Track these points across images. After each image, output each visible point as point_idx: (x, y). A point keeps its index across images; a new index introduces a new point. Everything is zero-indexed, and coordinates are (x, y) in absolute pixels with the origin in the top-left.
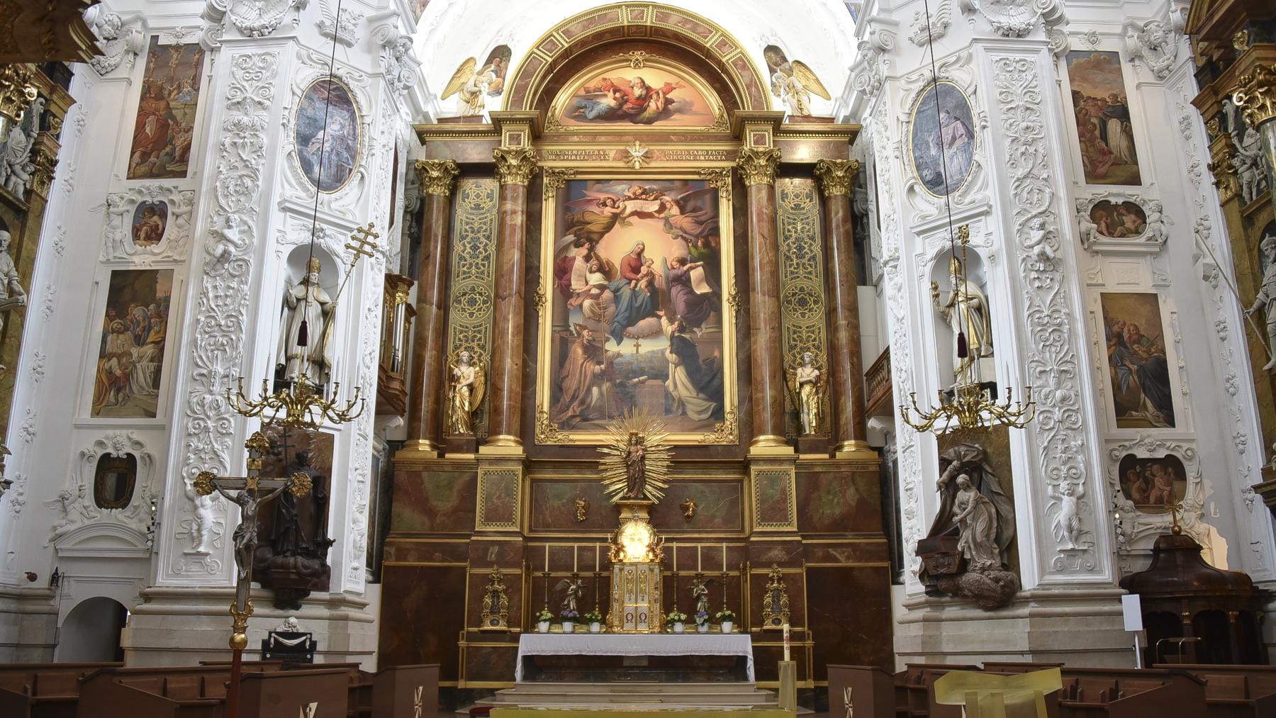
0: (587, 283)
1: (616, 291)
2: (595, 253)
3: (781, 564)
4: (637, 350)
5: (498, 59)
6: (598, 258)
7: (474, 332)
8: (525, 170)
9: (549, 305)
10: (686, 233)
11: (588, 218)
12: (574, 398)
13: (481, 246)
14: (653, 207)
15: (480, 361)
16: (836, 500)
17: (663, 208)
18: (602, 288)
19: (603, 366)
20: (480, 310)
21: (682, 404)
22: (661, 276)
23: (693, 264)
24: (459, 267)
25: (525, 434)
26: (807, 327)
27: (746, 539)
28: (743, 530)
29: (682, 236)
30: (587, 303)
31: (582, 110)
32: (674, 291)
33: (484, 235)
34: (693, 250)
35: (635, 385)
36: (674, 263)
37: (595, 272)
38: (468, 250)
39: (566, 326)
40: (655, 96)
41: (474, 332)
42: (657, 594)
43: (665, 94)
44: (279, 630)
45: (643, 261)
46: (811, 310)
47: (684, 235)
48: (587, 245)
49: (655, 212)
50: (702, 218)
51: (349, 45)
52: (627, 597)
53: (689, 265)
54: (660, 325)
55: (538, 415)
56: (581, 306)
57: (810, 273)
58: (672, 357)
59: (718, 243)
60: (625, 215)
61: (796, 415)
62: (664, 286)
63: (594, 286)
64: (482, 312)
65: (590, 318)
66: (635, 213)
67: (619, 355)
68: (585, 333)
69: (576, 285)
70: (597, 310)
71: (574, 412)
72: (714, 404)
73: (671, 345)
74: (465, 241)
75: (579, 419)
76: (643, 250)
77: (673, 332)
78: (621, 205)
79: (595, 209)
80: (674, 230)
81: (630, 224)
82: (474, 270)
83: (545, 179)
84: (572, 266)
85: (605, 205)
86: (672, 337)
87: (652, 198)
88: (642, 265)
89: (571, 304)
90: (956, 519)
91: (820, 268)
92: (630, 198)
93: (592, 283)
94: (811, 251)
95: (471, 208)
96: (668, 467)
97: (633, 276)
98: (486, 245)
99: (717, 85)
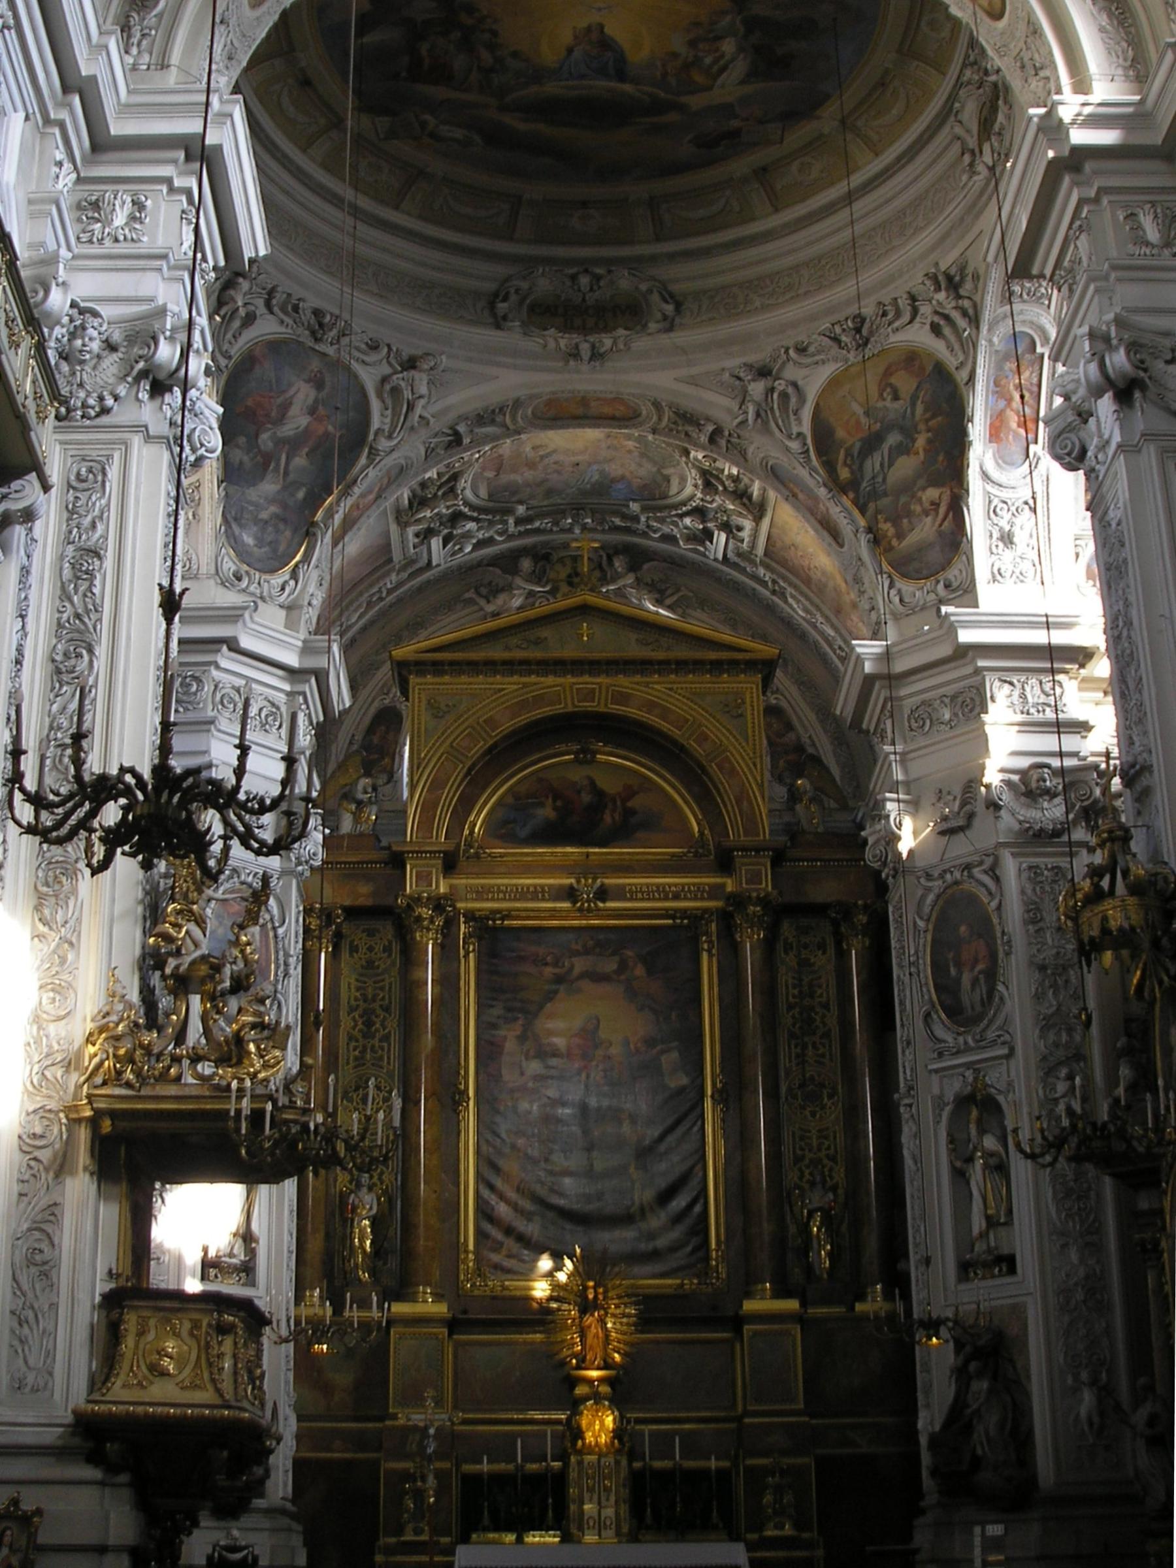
0: (522, 1074)
5: (383, 728)
8: (439, 922)
9: (471, 1103)
14: (610, 966)
15: (382, 1183)
17: (623, 966)
25: (448, 1289)
26: (819, 1131)
28: (734, 1405)
31: (511, 826)
36: (639, 1045)
38: (360, 1026)
40: (610, 805)
42: (625, 1493)
43: (624, 801)
44: (222, 1543)
57: (823, 1056)
66: (585, 975)
74: (356, 1014)
90: (969, 1411)
92: (577, 953)
96: (634, 1325)
98: (385, 1019)
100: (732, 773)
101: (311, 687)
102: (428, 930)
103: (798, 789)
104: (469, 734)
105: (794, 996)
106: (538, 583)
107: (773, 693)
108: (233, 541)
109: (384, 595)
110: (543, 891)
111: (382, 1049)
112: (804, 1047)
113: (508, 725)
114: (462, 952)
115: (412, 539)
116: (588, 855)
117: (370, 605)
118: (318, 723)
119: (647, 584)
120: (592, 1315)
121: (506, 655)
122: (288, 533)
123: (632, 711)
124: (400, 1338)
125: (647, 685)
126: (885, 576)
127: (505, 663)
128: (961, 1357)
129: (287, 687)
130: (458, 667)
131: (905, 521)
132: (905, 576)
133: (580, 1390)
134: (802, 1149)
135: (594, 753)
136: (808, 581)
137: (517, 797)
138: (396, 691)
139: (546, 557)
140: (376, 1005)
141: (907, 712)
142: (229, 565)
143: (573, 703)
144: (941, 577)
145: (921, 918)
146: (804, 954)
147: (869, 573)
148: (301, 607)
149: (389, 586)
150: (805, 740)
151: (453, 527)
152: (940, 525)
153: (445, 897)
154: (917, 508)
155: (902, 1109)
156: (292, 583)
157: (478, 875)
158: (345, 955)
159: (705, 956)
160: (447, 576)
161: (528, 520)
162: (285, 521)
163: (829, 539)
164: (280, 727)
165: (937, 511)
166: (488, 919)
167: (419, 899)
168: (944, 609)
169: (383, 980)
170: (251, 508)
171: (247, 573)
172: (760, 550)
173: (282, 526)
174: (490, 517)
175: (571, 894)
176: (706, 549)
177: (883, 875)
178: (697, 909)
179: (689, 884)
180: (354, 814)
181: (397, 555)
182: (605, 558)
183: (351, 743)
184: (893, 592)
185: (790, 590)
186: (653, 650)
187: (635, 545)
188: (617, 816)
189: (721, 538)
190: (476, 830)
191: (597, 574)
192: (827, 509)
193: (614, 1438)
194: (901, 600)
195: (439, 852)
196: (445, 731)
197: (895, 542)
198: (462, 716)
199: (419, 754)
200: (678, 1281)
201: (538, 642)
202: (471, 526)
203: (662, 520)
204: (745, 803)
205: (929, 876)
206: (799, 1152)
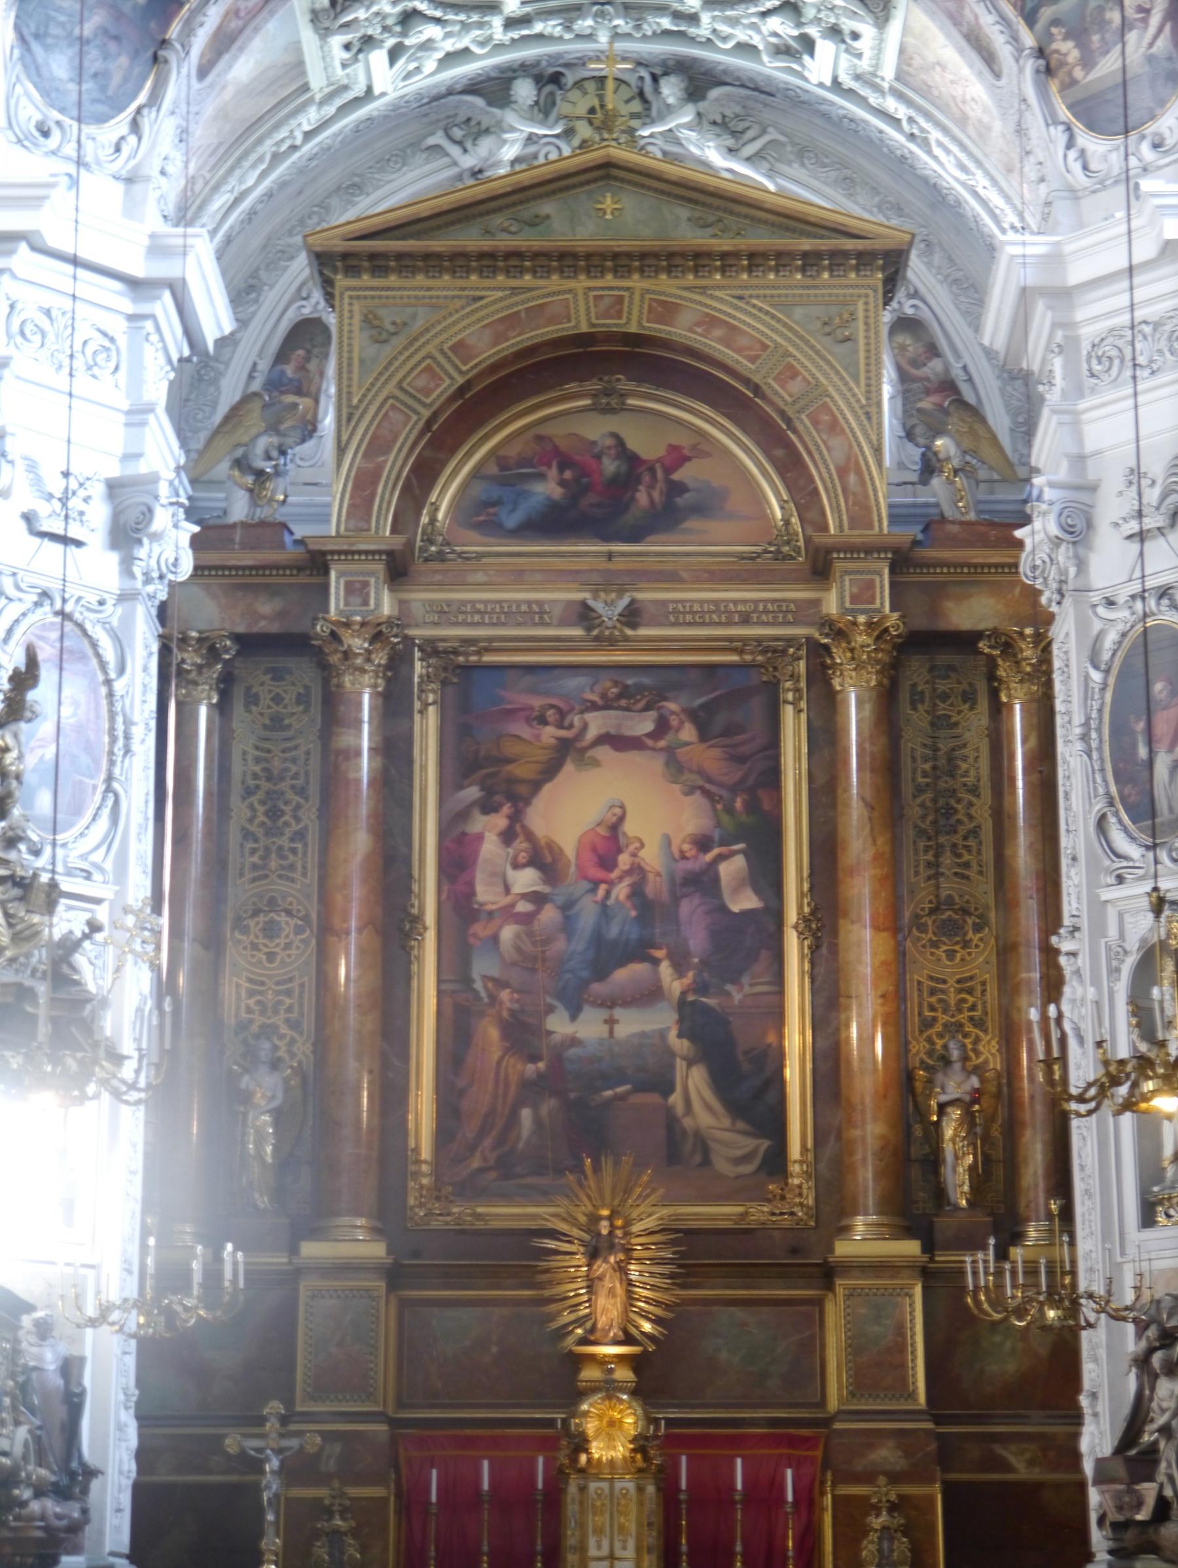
0: (507, 889)
1: (566, 907)
2: (524, 827)
3: (895, 1478)
4: (611, 1032)
5: (301, 352)
6: (530, 836)
7: (279, 993)
8: (381, 658)
10: (710, 780)
11: (510, 749)
12: (482, 1133)
13: (287, 809)
14: (644, 725)
15: (292, 1055)
16: (1008, 1345)
17: (662, 727)
18: (538, 899)
19: (541, 1065)
20: (287, 946)
21: (702, 1144)
22: (658, 874)
23: (723, 850)
24: (242, 856)
26: (959, 981)
27: (827, 1422)
29: (702, 788)
30: (508, 933)
31: (492, 510)
32: (686, 907)
33: (293, 787)
34: (725, 818)
35: (608, 1103)
36: (686, 847)
37: (525, 866)
38: (261, 818)
39: (467, 981)
40: (646, 478)
41: (279, 993)
45: (622, 841)
46: (966, 944)
47: (708, 786)
48: (506, 809)
49: (649, 735)
50: (745, 749)
51: (78, 544)
52: (592, 1542)
53: (716, 851)
54: (659, 980)
55: (412, 1168)
56: (495, 938)
57: (967, 865)
58: (681, 1046)
59: (778, 802)
60: (585, 743)
61: (934, 1162)
62: (665, 896)
63: (524, 896)
64: (294, 952)
65: (514, 964)
66: (606, 739)
67: (574, 1041)
68: (505, 995)
69: (486, 894)
70: (528, 947)
71: (485, 1159)
72: (765, 1144)
73: (681, 1021)
74: (254, 799)
75: (493, 1175)
76: (622, 819)
77: (684, 993)
78: (577, 720)
79: (523, 730)
80: (687, 776)
81: (596, 763)
82: (273, 864)
83: (418, 666)
84: (476, 853)
85: (543, 721)
86: (682, 1005)
87: (640, 705)
88: (619, 851)
89: (475, 935)
91: (988, 854)
92: (594, 707)
93: (517, 889)
94: (971, 818)
95: (265, 727)
96: (672, 1276)
97: (599, 874)
99: (779, 453)
100: (834, 427)
101: (164, 307)
102: (363, 671)
103: (936, 454)
104: (428, 369)
105: (925, 774)
106: (543, 123)
107: (911, 296)
108: (35, 71)
109: (298, 142)
110: (542, 613)
111: (294, 851)
112: (939, 851)
113: (487, 352)
114: (417, 705)
115: (340, 54)
116: (610, 556)
117: (277, 158)
118: (181, 360)
119: (714, 123)
120: (606, 1261)
121: (486, 244)
122: (124, 61)
123: (681, 330)
124: (313, 1297)
125: (703, 290)
126: (1061, 128)
127: (482, 256)
128: (1143, 1344)
129: (129, 307)
130: (406, 263)
131: (1096, 38)
132: (1092, 126)
133: (590, 1374)
134: (932, 1008)
135: (623, 395)
136: (963, 120)
137: (503, 464)
138: (317, 295)
139: (556, 79)
140: (283, 786)
141: (1085, 347)
142: (31, 110)
143: (589, 320)
144: (1151, 129)
145: (1096, 667)
146: (942, 708)
147: (1035, 120)
148: (147, 179)
149: (307, 128)
150: (957, 373)
151: (404, 34)
152: (1151, 45)
153: (389, 622)
154: (1114, 16)
155: (1063, 960)
156: (133, 139)
157: (441, 585)
158: (238, 709)
159: (788, 712)
160: (399, 114)
161: (525, 20)
162: (117, 38)
163: (979, 64)
164: (117, 368)
165: (1145, 21)
166: (456, 652)
167: (347, 625)
168: (1146, 185)
169: (296, 748)
170: (62, 18)
171: (58, 123)
172: (888, 71)
173: (113, 47)
174: (462, 17)
175: (584, 615)
176: (803, 66)
177: (1044, 600)
178: (777, 639)
179: (766, 601)
180: (251, 491)
181: (317, 82)
182: (648, 79)
183: (251, 377)
184: (1072, 154)
185: (935, 135)
186: (714, 236)
187: (695, 60)
188: (656, 495)
189: (825, 48)
190: (440, 516)
191: (636, 106)
192: (976, 17)
193: (634, 1450)
194: (1085, 168)
195: (380, 552)
196: (390, 363)
197: (1078, 73)
198: (416, 339)
199: (349, 400)
200: (741, 1209)
201: (535, 222)
202: (432, 31)
203: (734, 22)
204: (852, 478)
205: (1110, 603)
206: (927, 1013)
